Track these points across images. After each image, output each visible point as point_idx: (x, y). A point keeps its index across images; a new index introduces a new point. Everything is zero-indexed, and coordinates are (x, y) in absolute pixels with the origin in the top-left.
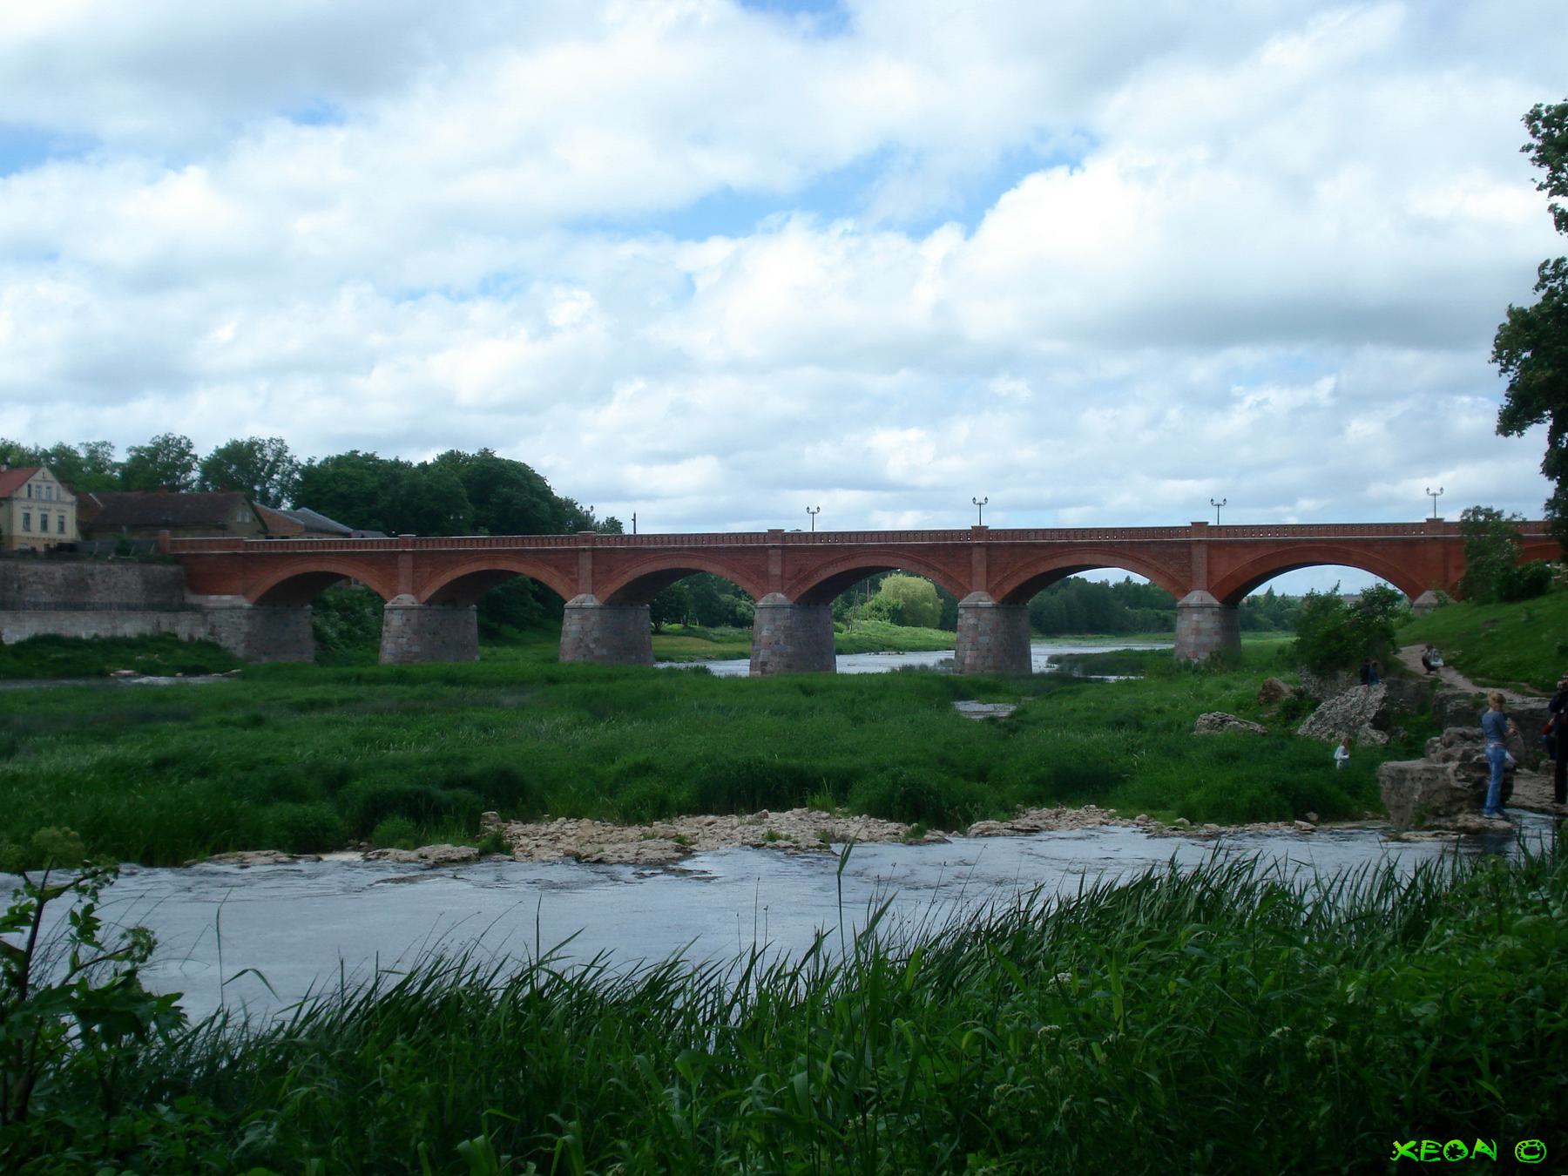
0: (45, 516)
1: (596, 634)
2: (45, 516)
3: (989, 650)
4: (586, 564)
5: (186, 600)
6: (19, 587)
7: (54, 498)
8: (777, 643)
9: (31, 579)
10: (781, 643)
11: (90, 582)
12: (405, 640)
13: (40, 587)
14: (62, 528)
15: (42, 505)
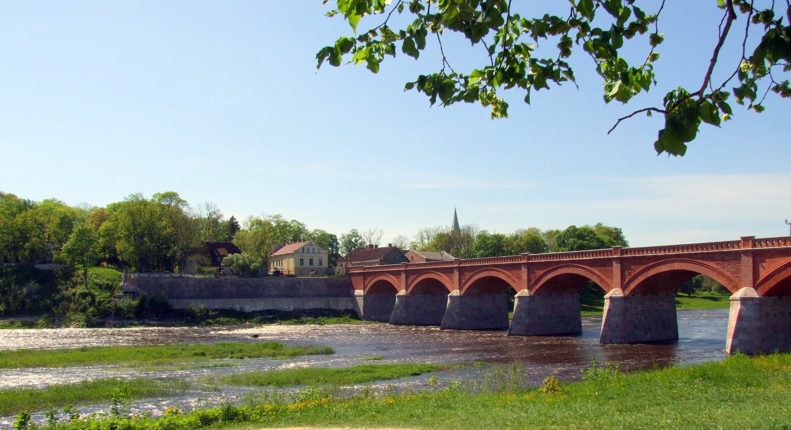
0: (303, 259)
1: (457, 310)
2: (303, 259)
3: (617, 327)
4: (616, 268)
5: (350, 292)
6: (264, 289)
7: (316, 251)
8: (520, 318)
9: (269, 285)
10: (523, 318)
11: (298, 286)
12: (399, 311)
13: (273, 288)
14: (321, 263)
15: (310, 255)
